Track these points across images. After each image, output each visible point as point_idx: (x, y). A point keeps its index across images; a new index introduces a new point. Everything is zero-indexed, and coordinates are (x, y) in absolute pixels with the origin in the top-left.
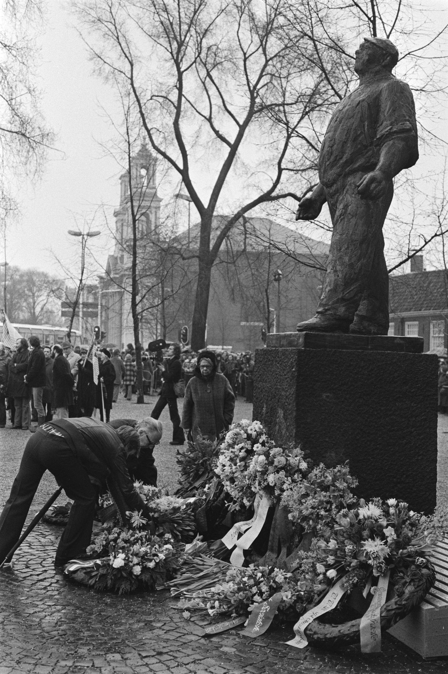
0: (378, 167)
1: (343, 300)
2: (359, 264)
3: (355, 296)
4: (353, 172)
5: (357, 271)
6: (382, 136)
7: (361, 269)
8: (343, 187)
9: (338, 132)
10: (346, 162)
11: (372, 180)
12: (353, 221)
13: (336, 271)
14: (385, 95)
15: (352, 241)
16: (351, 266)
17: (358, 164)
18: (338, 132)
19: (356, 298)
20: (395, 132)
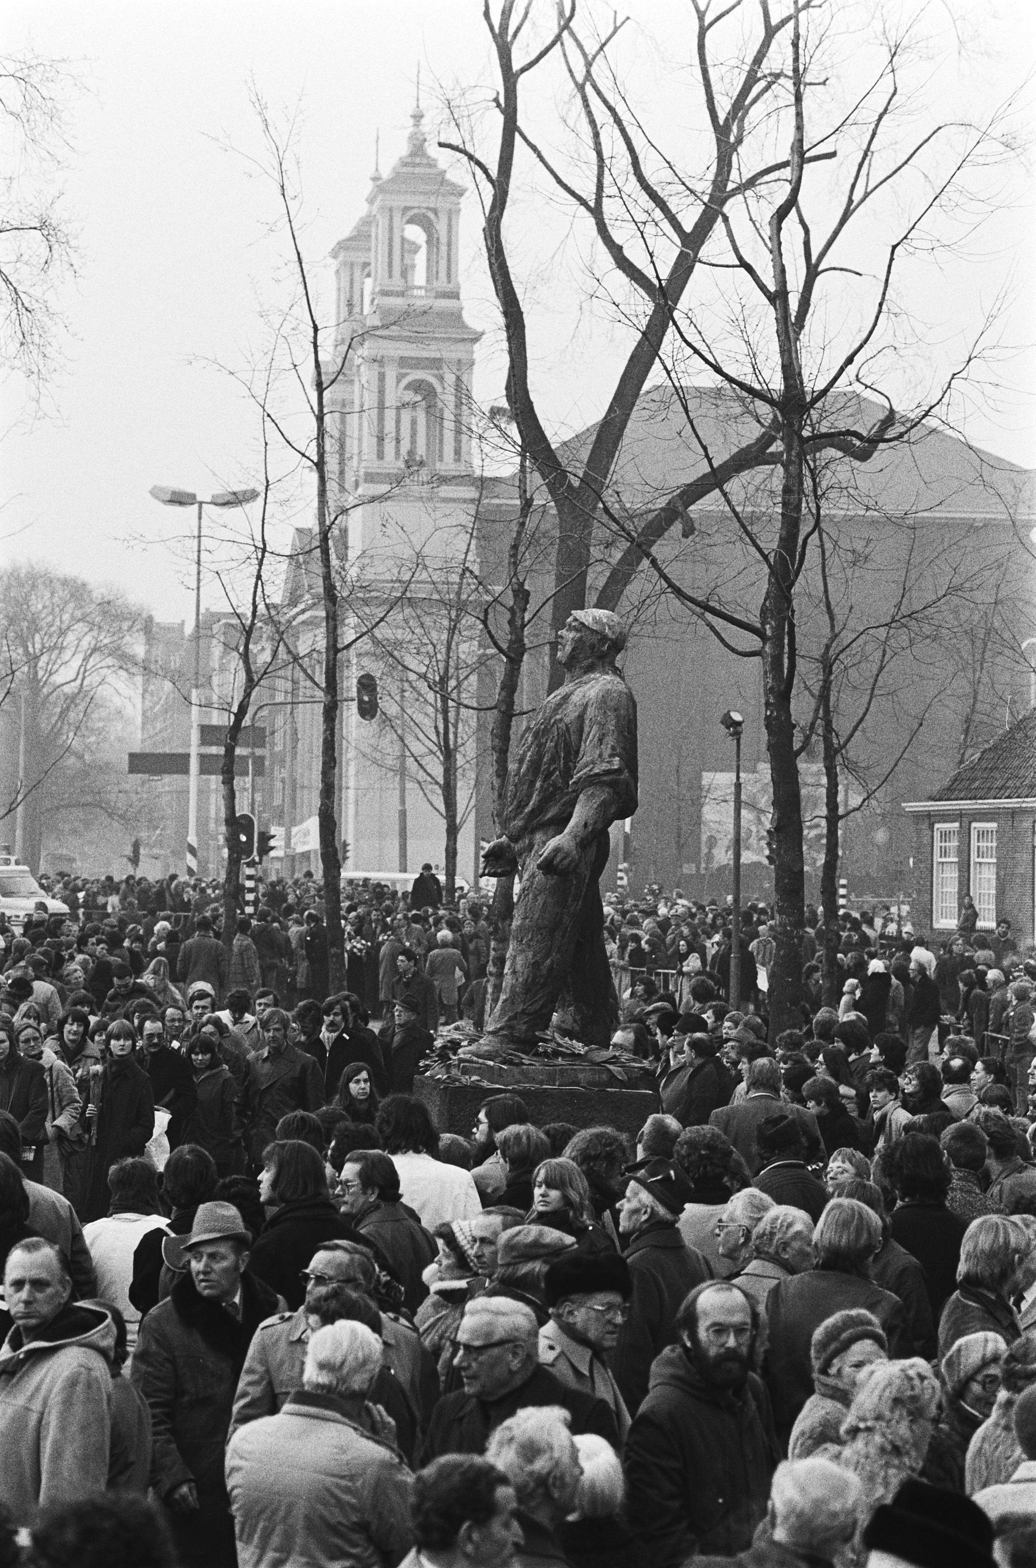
0: (566, 831)
1: (523, 1011)
2: (548, 961)
3: (541, 1009)
4: (543, 826)
5: (544, 972)
6: (580, 778)
7: (551, 969)
8: (531, 846)
9: (524, 766)
10: (532, 811)
11: (557, 850)
12: (540, 900)
13: (514, 972)
14: (591, 712)
15: (539, 929)
16: (536, 965)
17: (549, 815)
18: (524, 766)
19: (544, 1011)
20: (597, 774)
